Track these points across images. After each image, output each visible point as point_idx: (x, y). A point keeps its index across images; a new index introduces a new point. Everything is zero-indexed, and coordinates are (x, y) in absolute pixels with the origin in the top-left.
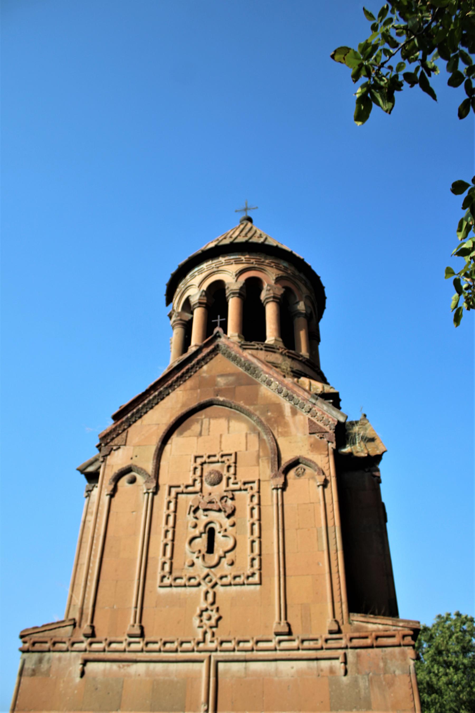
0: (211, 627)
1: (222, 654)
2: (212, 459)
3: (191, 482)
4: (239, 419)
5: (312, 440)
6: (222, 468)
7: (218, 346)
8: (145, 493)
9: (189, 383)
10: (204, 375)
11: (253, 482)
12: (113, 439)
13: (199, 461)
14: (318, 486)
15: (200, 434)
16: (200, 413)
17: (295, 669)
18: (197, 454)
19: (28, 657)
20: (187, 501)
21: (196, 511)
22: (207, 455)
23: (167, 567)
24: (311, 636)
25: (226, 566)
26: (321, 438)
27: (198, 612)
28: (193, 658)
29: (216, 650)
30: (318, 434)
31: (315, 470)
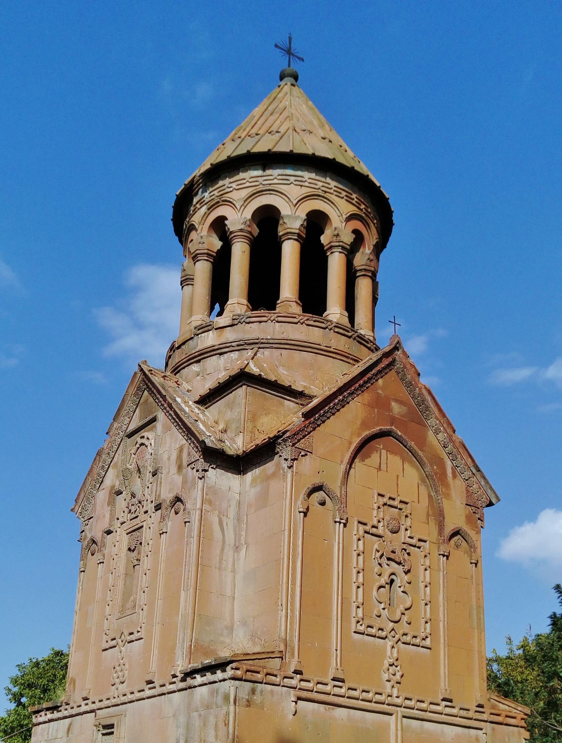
0: (398, 683)
2: (391, 502)
4: (411, 462)
5: (467, 512)
7: (394, 360)
8: (336, 522)
10: (380, 392)
11: (425, 541)
12: (299, 441)
13: (382, 500)
14: (471, 563)
15: (379, 469)
19: (241, 686)
24: (466, 707)
25: (405, 623)
26: (474, 513)
27: (387, 665)
28: (386, 711)
29: (400, 707)
30: (473, 508)
31: (471, 547)
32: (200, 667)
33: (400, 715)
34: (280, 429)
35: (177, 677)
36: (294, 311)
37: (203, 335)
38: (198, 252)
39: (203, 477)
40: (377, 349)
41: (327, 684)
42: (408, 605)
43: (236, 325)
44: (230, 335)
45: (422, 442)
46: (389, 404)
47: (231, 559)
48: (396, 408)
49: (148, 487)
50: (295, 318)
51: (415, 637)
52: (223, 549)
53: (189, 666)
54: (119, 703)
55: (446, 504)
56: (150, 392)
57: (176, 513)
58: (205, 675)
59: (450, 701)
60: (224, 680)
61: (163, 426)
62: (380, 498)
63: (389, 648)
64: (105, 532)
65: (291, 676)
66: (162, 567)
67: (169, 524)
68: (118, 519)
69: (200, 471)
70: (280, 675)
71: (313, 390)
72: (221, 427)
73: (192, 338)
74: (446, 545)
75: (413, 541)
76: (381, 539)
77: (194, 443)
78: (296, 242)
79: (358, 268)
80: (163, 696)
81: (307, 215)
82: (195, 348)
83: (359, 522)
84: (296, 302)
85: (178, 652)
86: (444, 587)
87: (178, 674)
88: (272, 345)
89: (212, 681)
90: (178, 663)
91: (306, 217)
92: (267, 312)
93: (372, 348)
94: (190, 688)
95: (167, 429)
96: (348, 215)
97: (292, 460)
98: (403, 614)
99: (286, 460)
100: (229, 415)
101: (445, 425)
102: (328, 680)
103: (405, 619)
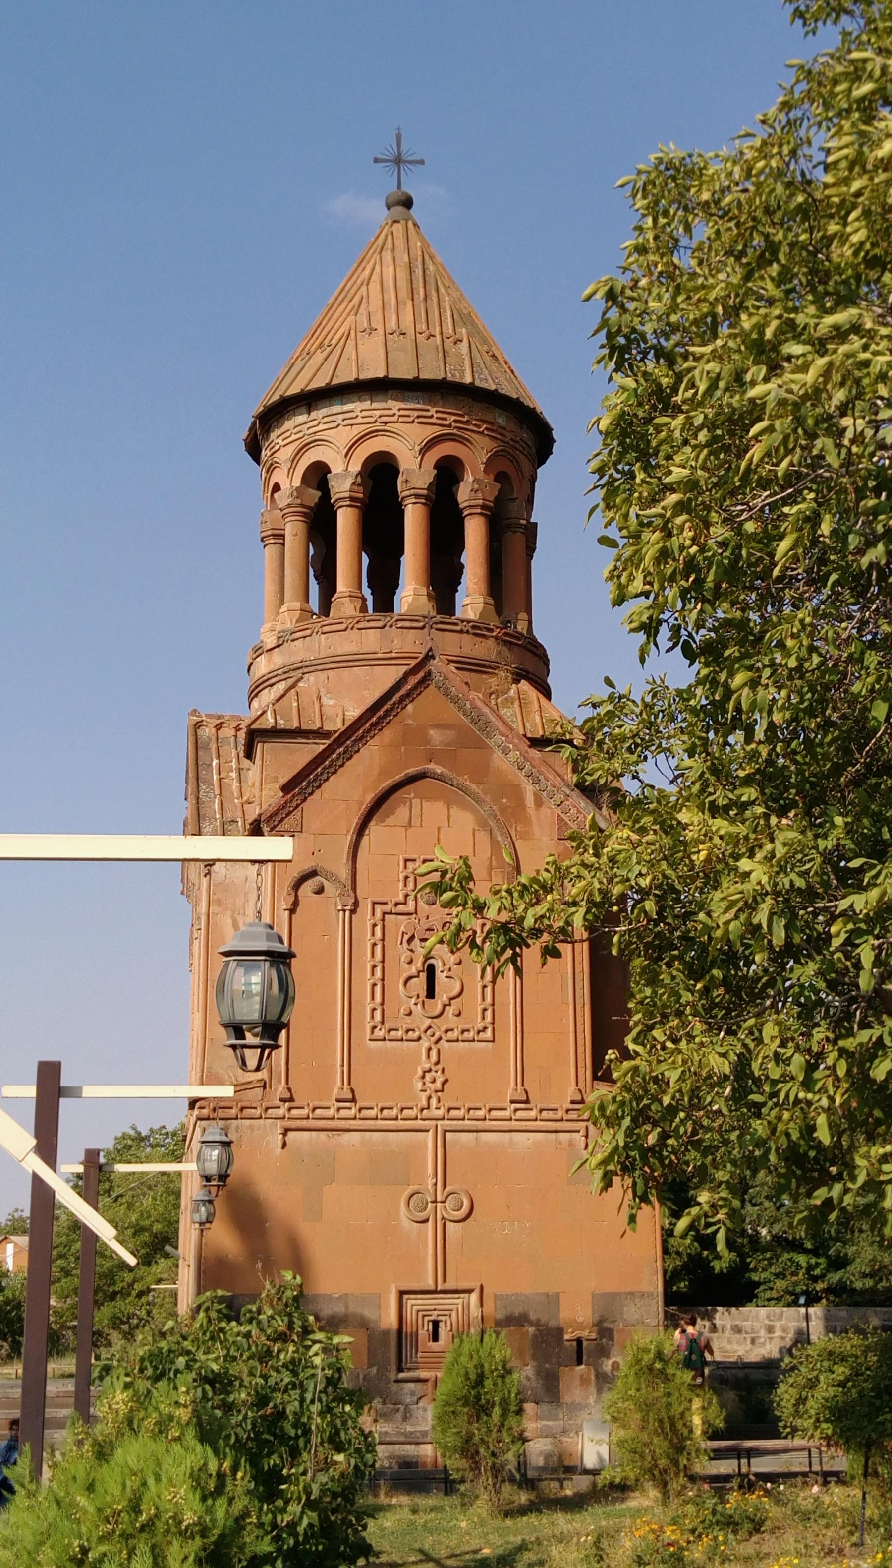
0: (436, 1091)
1: (450, 1122)
3: (401, 898)
7: (429, 673)
9: (387, 734)
10: (410, 722)
12: (282, 819)
16: (408, 787)
18: (407, 856)
20: (399, 925)
21: (410, 941)
22: (422, 858)
23: (378, 1015)
27: (420, 1073)
28: (418, 1128)
29: (443, 1119)
46: (426, 735)
48: (435, 735)
59: (527, 1101)
62: (409, 864)
79: (461, 506)
101: (516, 741)
103: (450, 1011)
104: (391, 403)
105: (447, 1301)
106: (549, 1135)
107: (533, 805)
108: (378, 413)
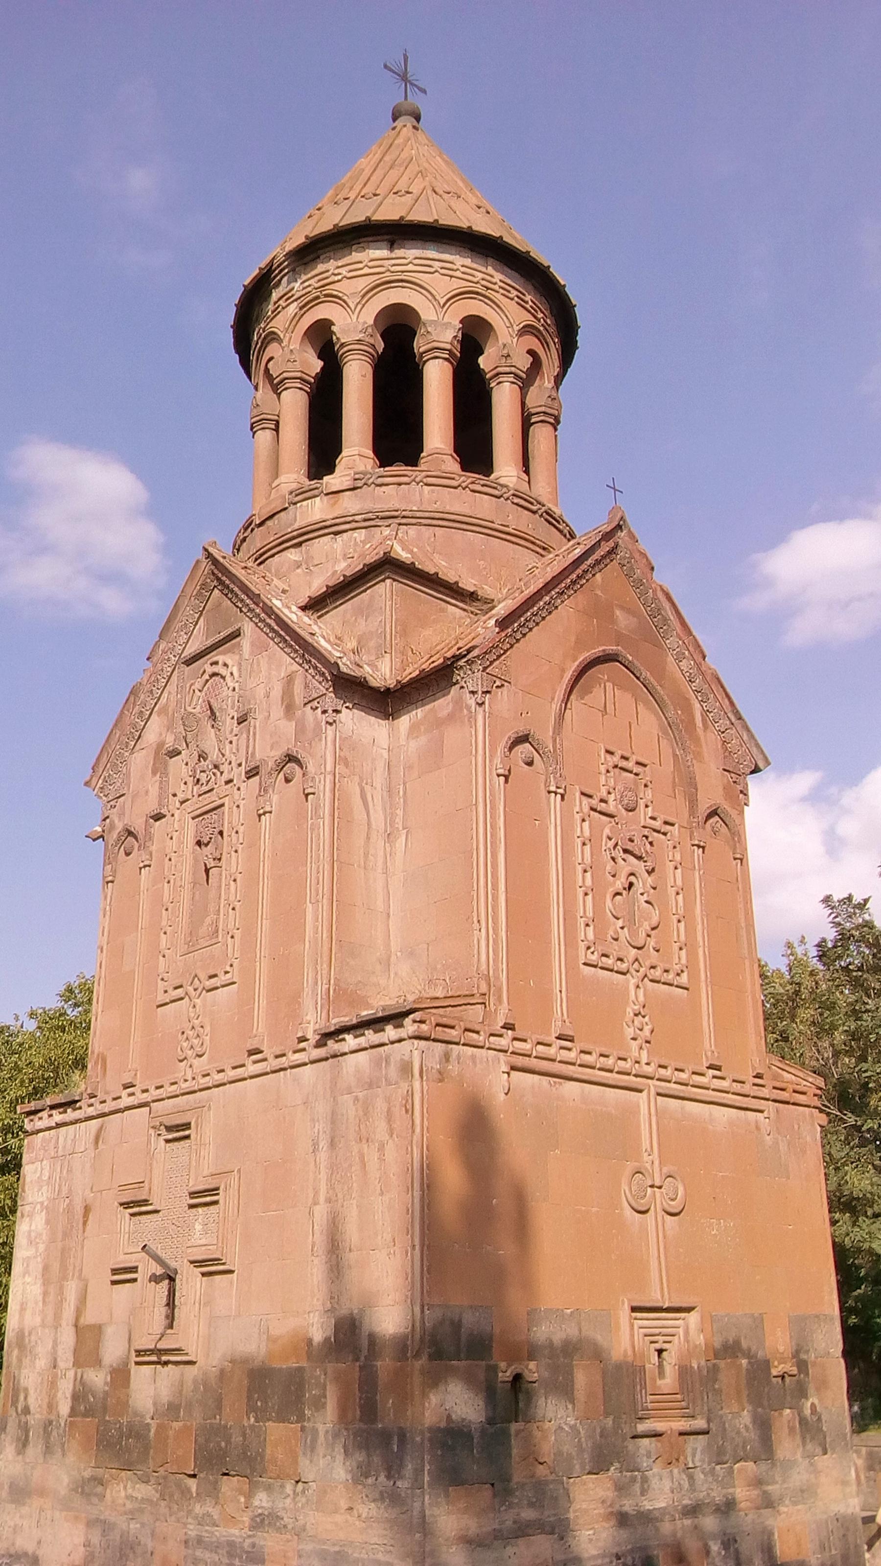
1: (658, 1083)
2: (623, 764)
4: (646, 703)
6: (636, 783)
7: (617, 545)
8: (549, 792)
10: (599, 593)
11: (673, 825)
12: (491, 663)
17: (725, 1119)
19: (428, 1049)
26: (735, 782)
27: (632, 1014)
28: (634, 1086)
29: (652, 1078)
30: (733, 775)
32: (354, 1021)
33: (653, 1092)
34: (460, 645)
35: (307, 1040)
36: (449, 469)
37: (305, 503)
38: (285, 375)
39: (335, 721)
40: (572, 536)
41: (549, 1045)
42: (654, 923)
43: (360, 488)
44: (350, 504)
45: (660, 672)
46: (613, 613)
47: (381, 853)
49: (231, 742)
50: (453, 479)
51: (666, 971)
52: (368, 838)
53: (333, 1022)
54: (196, 1088)
55: (697, 768)
56: (226, 591)
57: (287, 781)
58: (363, 1035)
59: (718, 1068)
60: (400, 1041)
61: (253, 644)
62: (608, 756)
63: (632, 988)
64: (151, 817)
65: (497, 1033)
66: (266, 868)
67: (275, 798)
68: (175, 795)
69: (330, 711)
70: (485, 1032)
71: (486, 591)
72: (352, 644)
73: (285, 509)
74: (701, 830)
75: (657, 824)
76: (612, 820)
77: (316, 668)
78: (446, 363)
79: (533, 411)
80: (282, 1073)
81: (461, 322)
82: (292, 525)
83: (583, 794)
84: (451, 455)
85: (308, 1002)
86: (701, 896)
87: (310, 1035)
88: (419, 520)
89: (377, 1043)
90: (308, 1018)
91: (461, 326)
92: (410, 468)
93: (566, 531)
94: (335, 1056)
95: (259, 648)
96: (521, 326)
97: (483, 692)
98: (649, 936)
99: (473, 692)
100: (362, 626)
102: (552, 1038)
104: (490, 270)
105: (669, 1321)
106: (743, 1112)
107: (701, 725)
108: (480, 275)
